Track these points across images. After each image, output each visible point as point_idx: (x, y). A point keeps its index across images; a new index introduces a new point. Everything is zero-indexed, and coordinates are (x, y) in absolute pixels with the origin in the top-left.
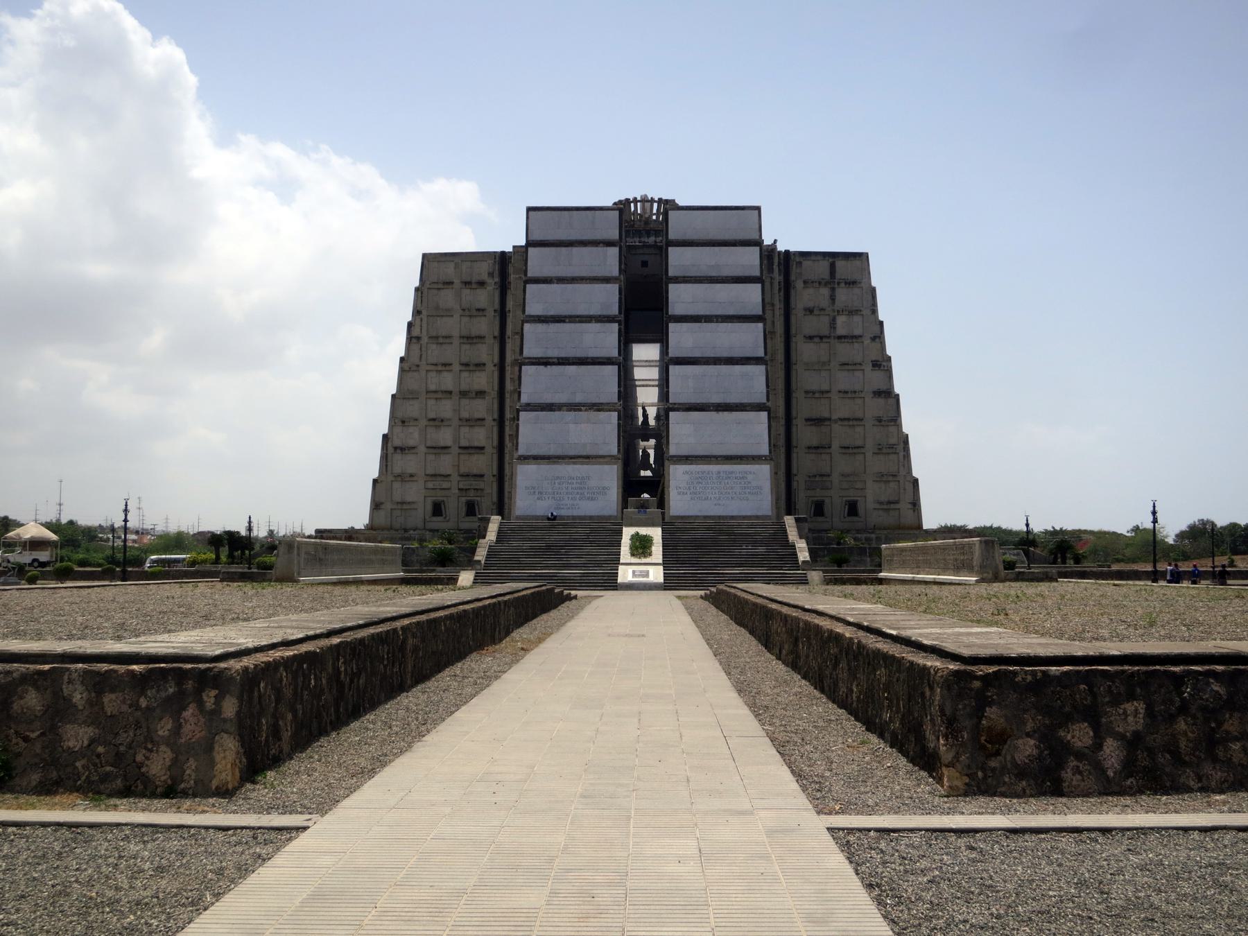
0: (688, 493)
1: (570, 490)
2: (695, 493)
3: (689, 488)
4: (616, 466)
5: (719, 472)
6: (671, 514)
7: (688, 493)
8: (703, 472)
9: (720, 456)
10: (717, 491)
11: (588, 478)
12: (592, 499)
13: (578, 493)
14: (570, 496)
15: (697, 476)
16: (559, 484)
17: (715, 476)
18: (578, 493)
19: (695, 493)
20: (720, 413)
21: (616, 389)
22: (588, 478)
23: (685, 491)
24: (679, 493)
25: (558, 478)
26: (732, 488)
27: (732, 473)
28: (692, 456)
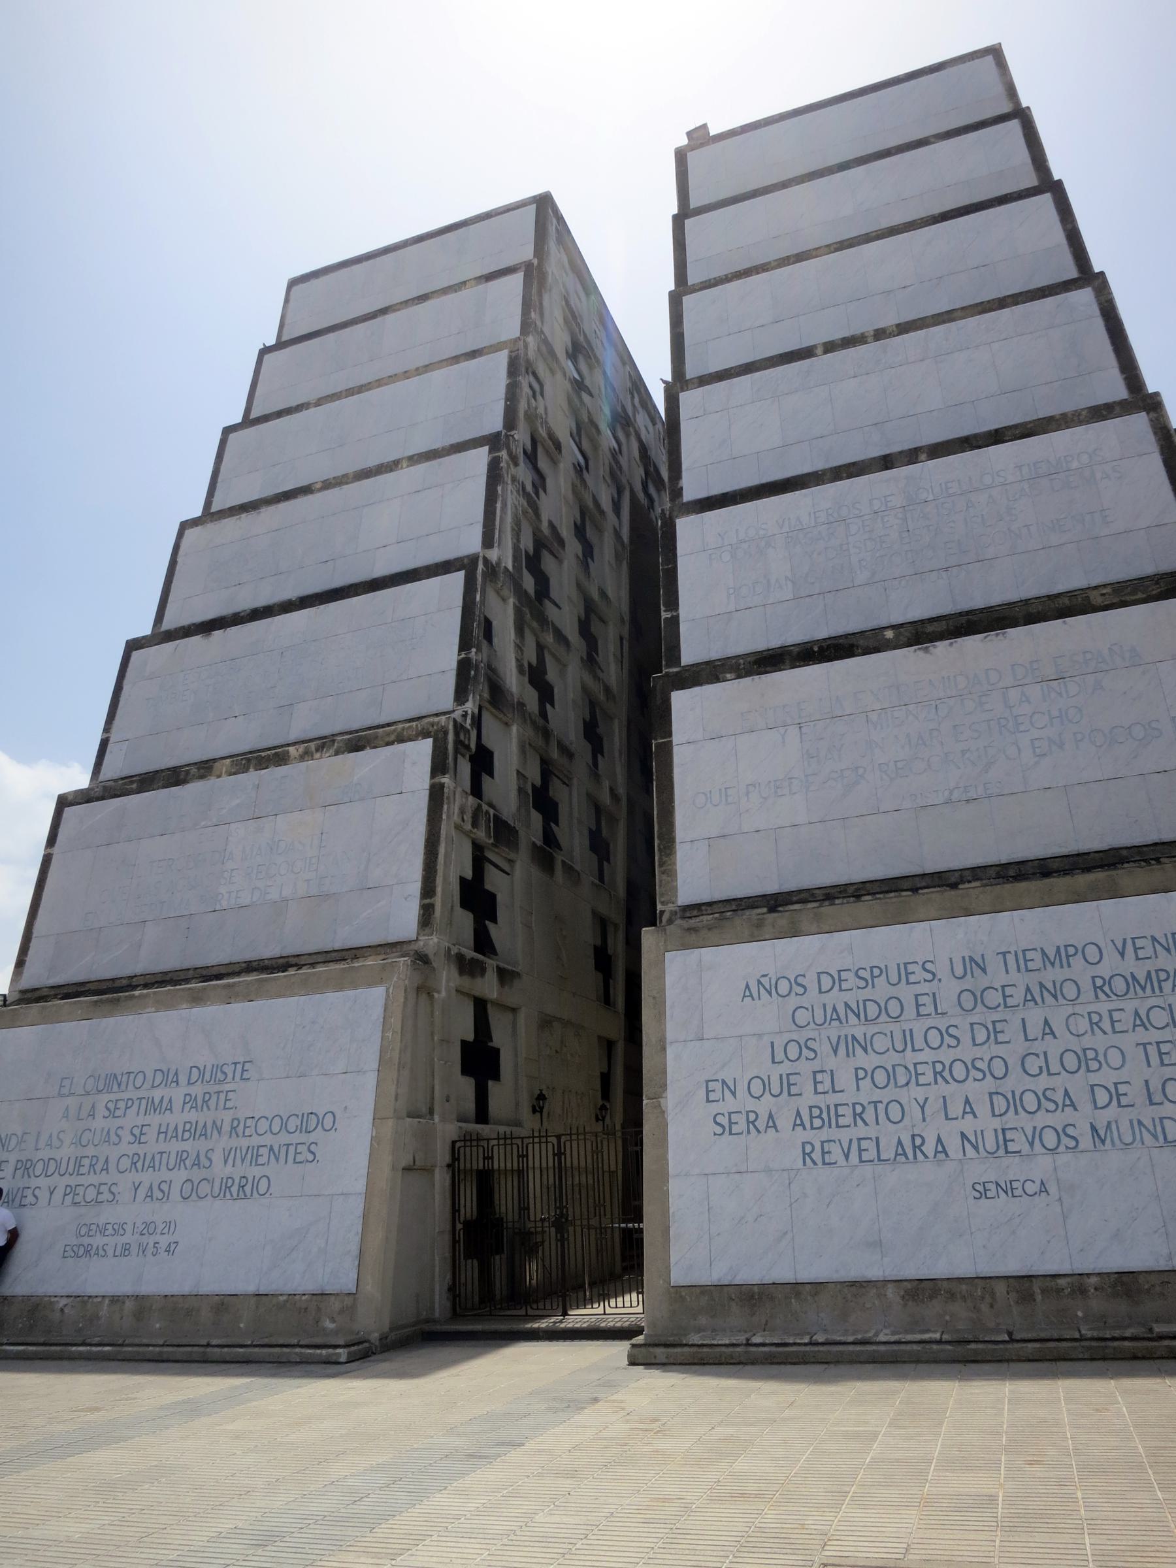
0: (785, 1121)
1: (152, 1146)
2: (828, 1117)
3: (788, 1085)
4: (377, 994)
5: (976, 964)
6: (678, 1277)
7: (785, 1121)
8: (870, 976)
9: (977, 873)
10: (977, 1090)
11: (242, 1068)
12: (243, 1189)
13: (181, 1159)
14: (147, 1177)
15: (836, 998)
16: (112, 1113)
17: (949, 990)
18: (181, 1159)
19: (828, 1117)
20: (941, 646)
21: (449, 657)
22: (242, 1068)
23: (764, 1106)
24: (726, 1128)
25: (113, 1081)
26: (1085, 1060)
27: (1063, 956)
28: (805, 896)
